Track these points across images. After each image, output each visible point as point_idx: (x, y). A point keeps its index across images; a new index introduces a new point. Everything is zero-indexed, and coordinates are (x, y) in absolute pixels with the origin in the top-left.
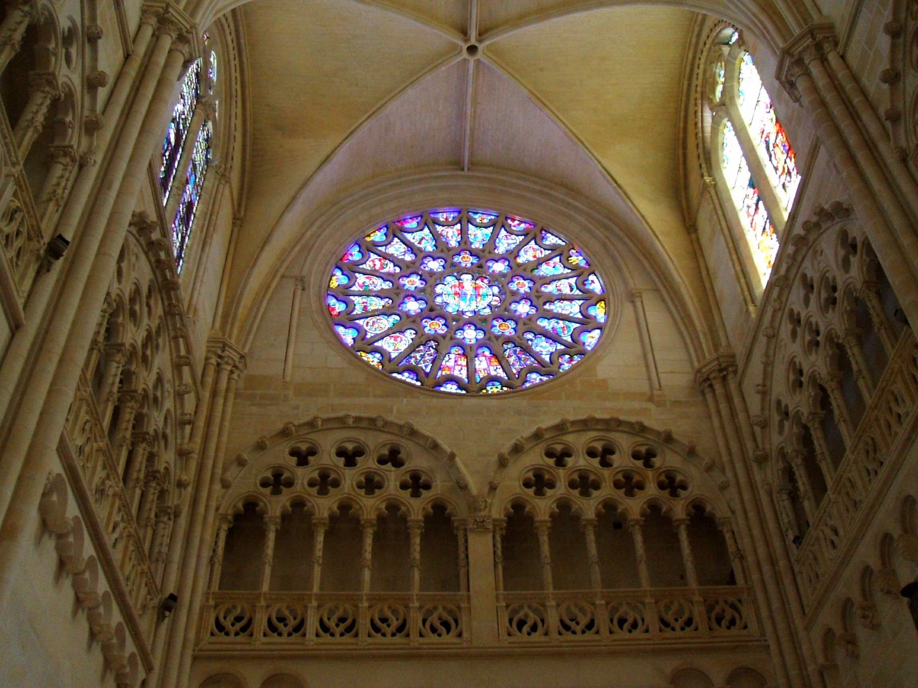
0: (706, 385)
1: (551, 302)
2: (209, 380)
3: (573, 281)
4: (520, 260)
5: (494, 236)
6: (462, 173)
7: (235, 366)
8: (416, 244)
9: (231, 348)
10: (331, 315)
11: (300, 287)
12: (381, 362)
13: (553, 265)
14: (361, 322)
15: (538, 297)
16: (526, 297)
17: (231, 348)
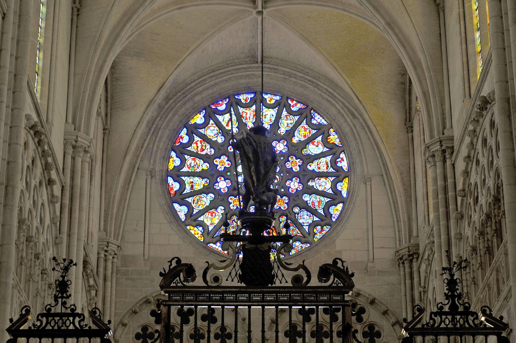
0: (401, 262)
1: (313, 179)
2: (101, 270)
3: (329, 158)
4: (295, 140)
5: (278, 117)
6: (257, 65)
7: (115, 254)
8: (225, 125)
9: (112, 243)
10: (170, 194)
11: (150, 177)
12: (202, 234)
13: (316, 144)
14: (190, 200)
15: (304, 176)
16: (296, 175)
17: (112, 243)
